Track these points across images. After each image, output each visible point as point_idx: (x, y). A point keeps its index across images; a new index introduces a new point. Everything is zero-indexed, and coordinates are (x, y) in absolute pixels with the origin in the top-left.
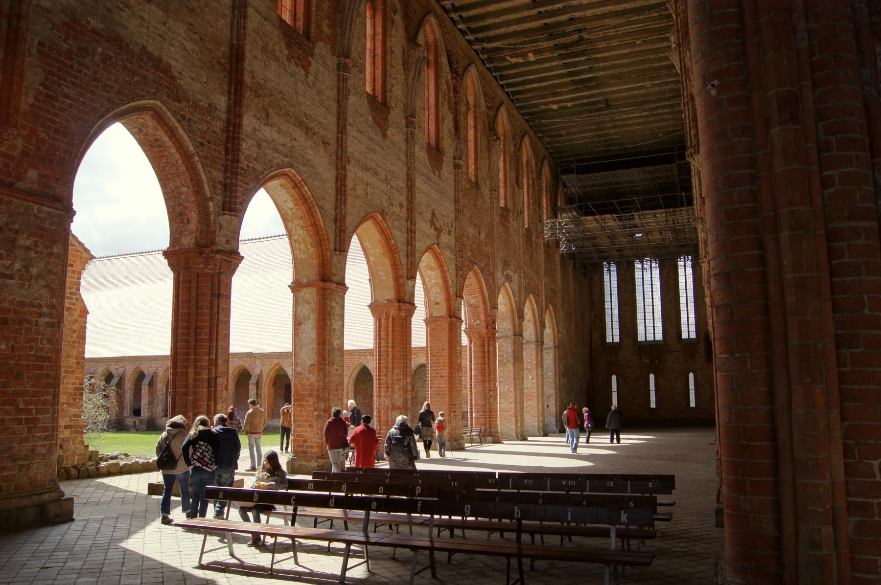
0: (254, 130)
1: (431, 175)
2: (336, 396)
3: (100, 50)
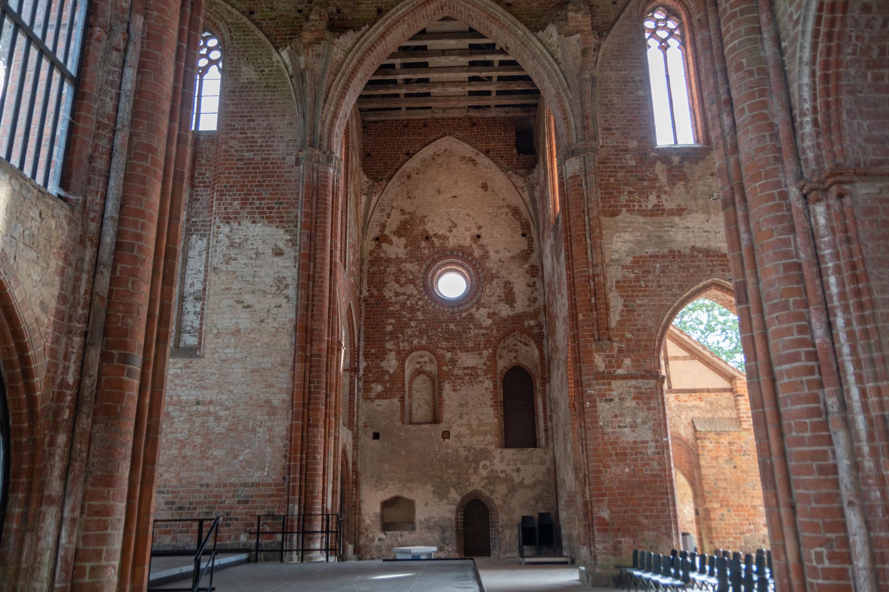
3: (658, 266)
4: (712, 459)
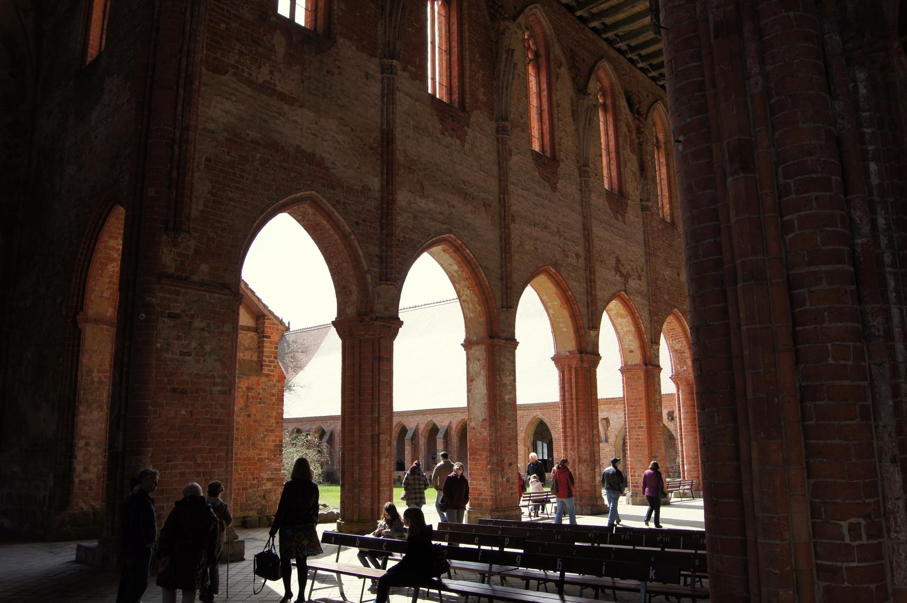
0: (410, 203)
1: (614, 221)
2: (509, 449)
3: (258, 156)
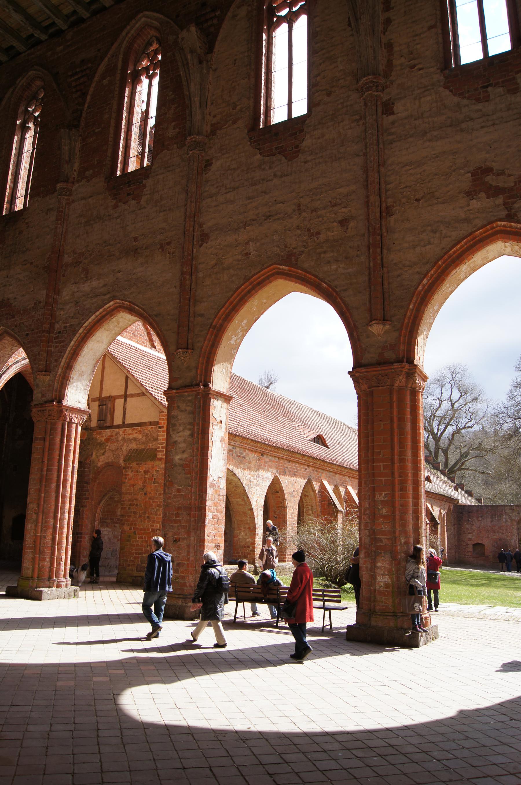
2: (176, 522)
4: (131, 486)
